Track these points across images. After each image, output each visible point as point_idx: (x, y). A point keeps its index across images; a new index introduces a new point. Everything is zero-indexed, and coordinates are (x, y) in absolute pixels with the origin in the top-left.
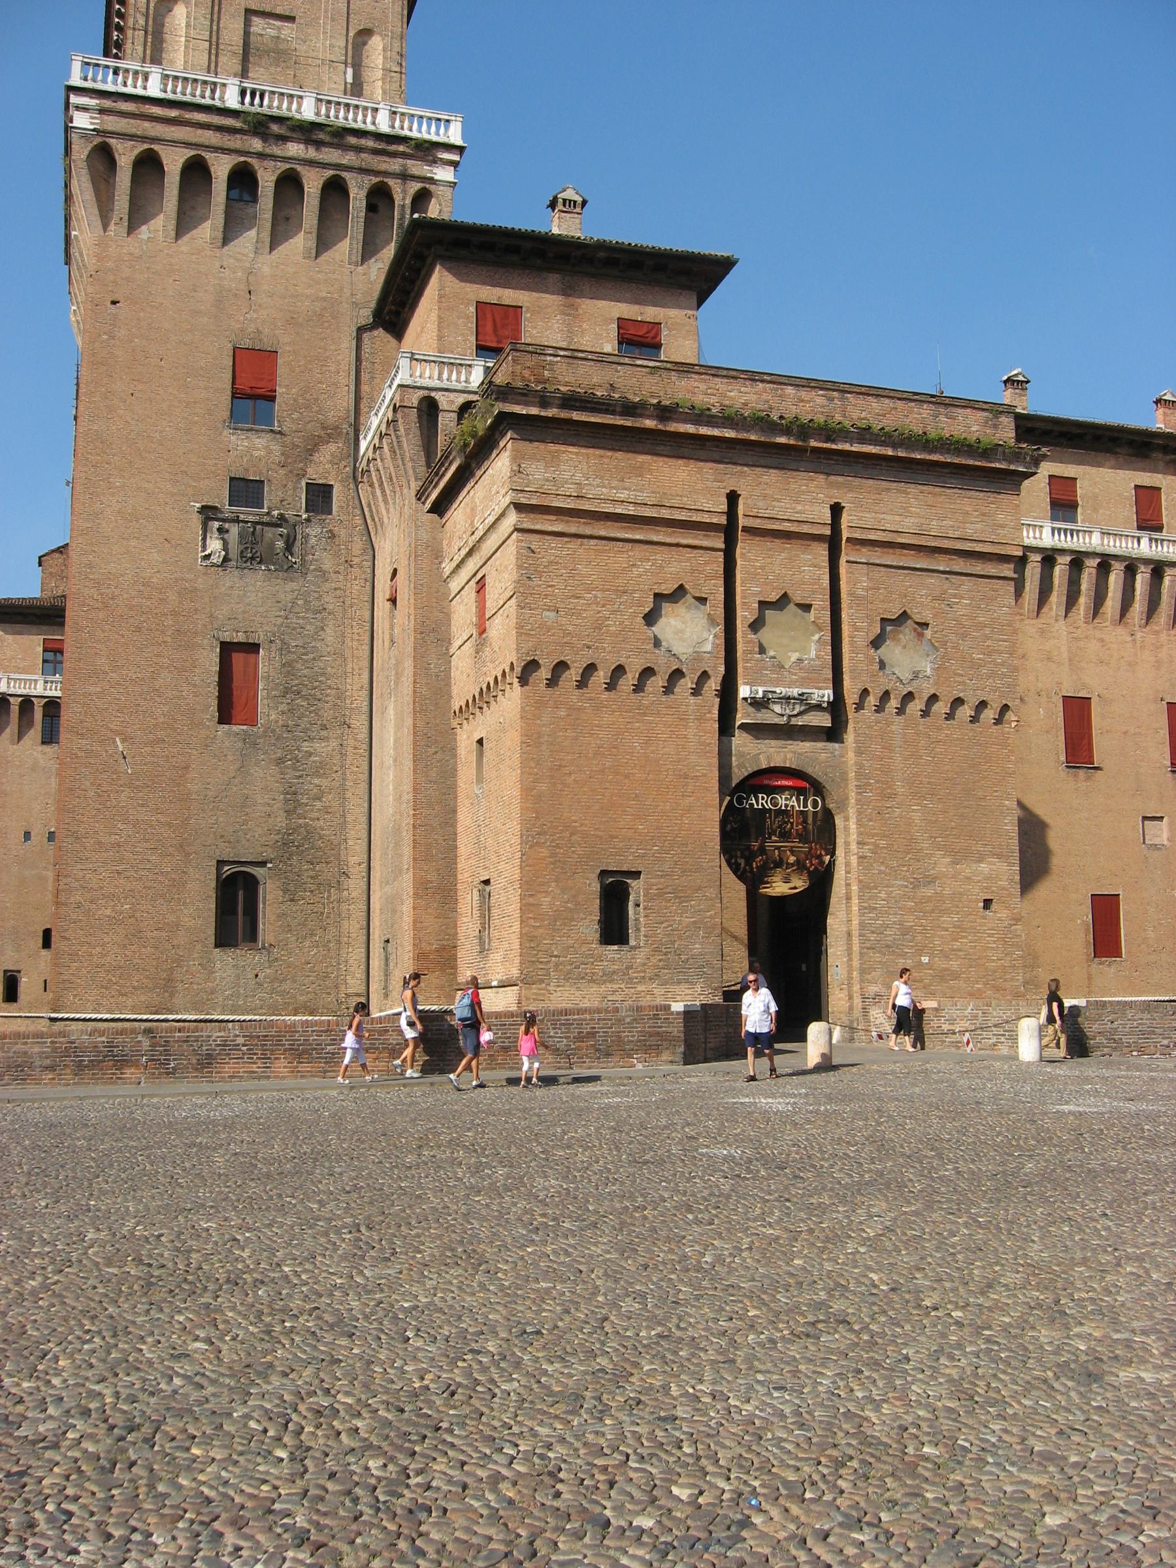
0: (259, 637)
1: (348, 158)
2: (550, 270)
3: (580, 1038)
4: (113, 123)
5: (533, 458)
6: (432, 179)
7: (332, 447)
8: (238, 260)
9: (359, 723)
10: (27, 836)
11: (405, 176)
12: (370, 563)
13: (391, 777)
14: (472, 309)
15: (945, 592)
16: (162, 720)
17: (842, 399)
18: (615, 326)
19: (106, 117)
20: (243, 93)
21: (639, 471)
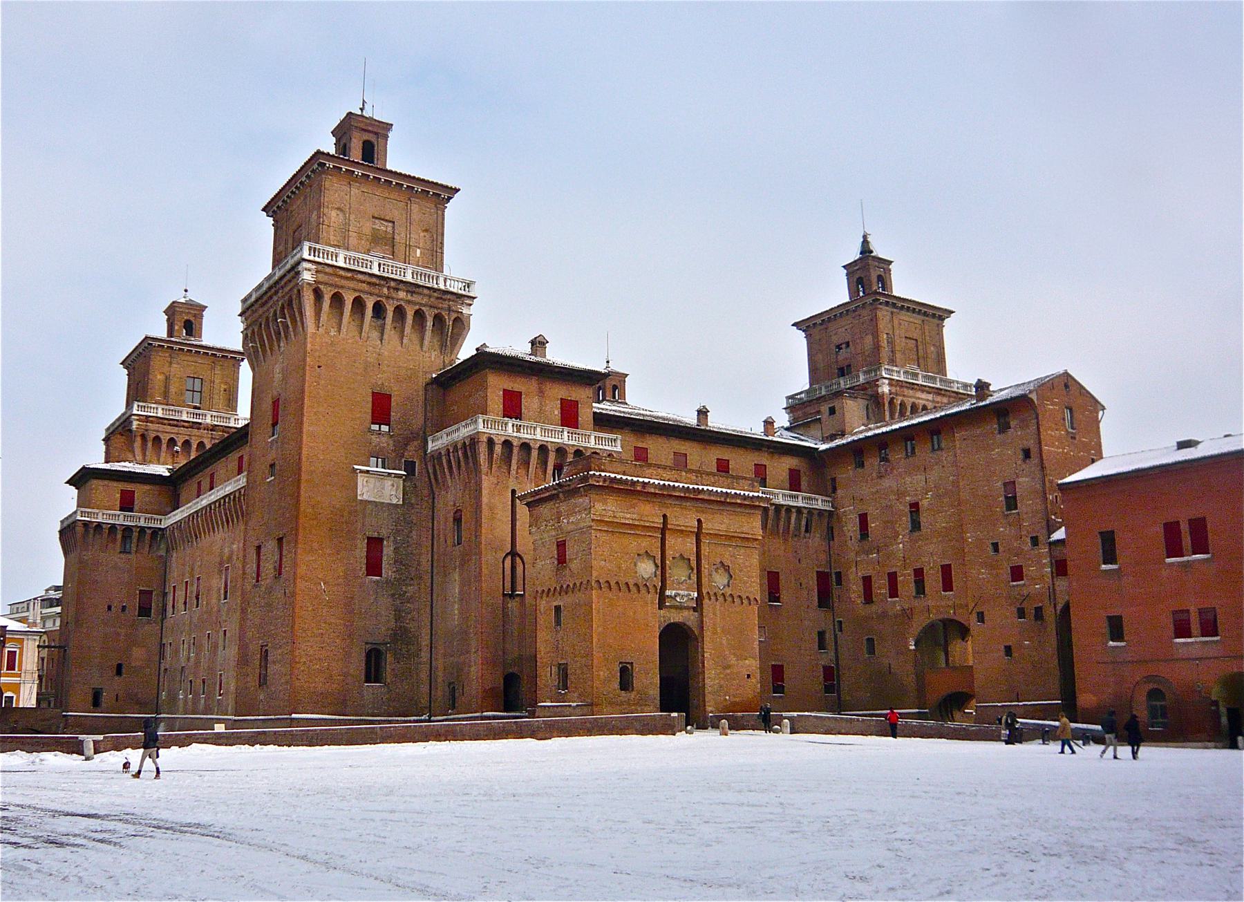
0: (384, 533)
1: (425, 301)
2: (533, 375)
3: (644, 725)
4: (322, 277)
5: (599, 501)
6: (462, 312)
7: (416, 443)
8: (374, 348)
9: (427, 578)
10: (109, 608)
11: (449, 310)
12: (430, 501)
13: (456, 607)
14: (501, 393)
15: (734, 553)
16: (341, 574)
17: (701, 477)
18: (559, 402)
19: (318, 274)
20: (380, 265)
21: (633, 506)
